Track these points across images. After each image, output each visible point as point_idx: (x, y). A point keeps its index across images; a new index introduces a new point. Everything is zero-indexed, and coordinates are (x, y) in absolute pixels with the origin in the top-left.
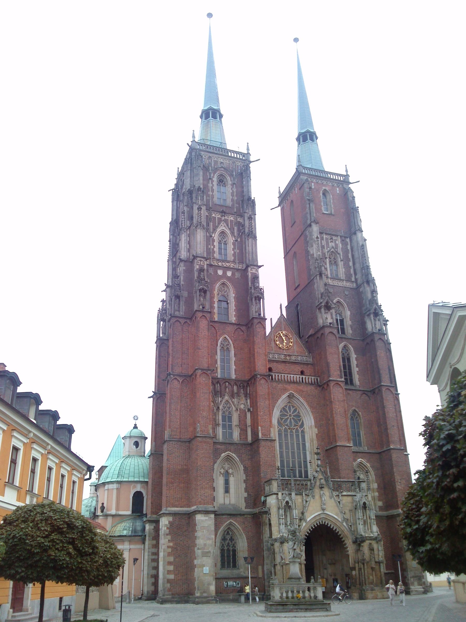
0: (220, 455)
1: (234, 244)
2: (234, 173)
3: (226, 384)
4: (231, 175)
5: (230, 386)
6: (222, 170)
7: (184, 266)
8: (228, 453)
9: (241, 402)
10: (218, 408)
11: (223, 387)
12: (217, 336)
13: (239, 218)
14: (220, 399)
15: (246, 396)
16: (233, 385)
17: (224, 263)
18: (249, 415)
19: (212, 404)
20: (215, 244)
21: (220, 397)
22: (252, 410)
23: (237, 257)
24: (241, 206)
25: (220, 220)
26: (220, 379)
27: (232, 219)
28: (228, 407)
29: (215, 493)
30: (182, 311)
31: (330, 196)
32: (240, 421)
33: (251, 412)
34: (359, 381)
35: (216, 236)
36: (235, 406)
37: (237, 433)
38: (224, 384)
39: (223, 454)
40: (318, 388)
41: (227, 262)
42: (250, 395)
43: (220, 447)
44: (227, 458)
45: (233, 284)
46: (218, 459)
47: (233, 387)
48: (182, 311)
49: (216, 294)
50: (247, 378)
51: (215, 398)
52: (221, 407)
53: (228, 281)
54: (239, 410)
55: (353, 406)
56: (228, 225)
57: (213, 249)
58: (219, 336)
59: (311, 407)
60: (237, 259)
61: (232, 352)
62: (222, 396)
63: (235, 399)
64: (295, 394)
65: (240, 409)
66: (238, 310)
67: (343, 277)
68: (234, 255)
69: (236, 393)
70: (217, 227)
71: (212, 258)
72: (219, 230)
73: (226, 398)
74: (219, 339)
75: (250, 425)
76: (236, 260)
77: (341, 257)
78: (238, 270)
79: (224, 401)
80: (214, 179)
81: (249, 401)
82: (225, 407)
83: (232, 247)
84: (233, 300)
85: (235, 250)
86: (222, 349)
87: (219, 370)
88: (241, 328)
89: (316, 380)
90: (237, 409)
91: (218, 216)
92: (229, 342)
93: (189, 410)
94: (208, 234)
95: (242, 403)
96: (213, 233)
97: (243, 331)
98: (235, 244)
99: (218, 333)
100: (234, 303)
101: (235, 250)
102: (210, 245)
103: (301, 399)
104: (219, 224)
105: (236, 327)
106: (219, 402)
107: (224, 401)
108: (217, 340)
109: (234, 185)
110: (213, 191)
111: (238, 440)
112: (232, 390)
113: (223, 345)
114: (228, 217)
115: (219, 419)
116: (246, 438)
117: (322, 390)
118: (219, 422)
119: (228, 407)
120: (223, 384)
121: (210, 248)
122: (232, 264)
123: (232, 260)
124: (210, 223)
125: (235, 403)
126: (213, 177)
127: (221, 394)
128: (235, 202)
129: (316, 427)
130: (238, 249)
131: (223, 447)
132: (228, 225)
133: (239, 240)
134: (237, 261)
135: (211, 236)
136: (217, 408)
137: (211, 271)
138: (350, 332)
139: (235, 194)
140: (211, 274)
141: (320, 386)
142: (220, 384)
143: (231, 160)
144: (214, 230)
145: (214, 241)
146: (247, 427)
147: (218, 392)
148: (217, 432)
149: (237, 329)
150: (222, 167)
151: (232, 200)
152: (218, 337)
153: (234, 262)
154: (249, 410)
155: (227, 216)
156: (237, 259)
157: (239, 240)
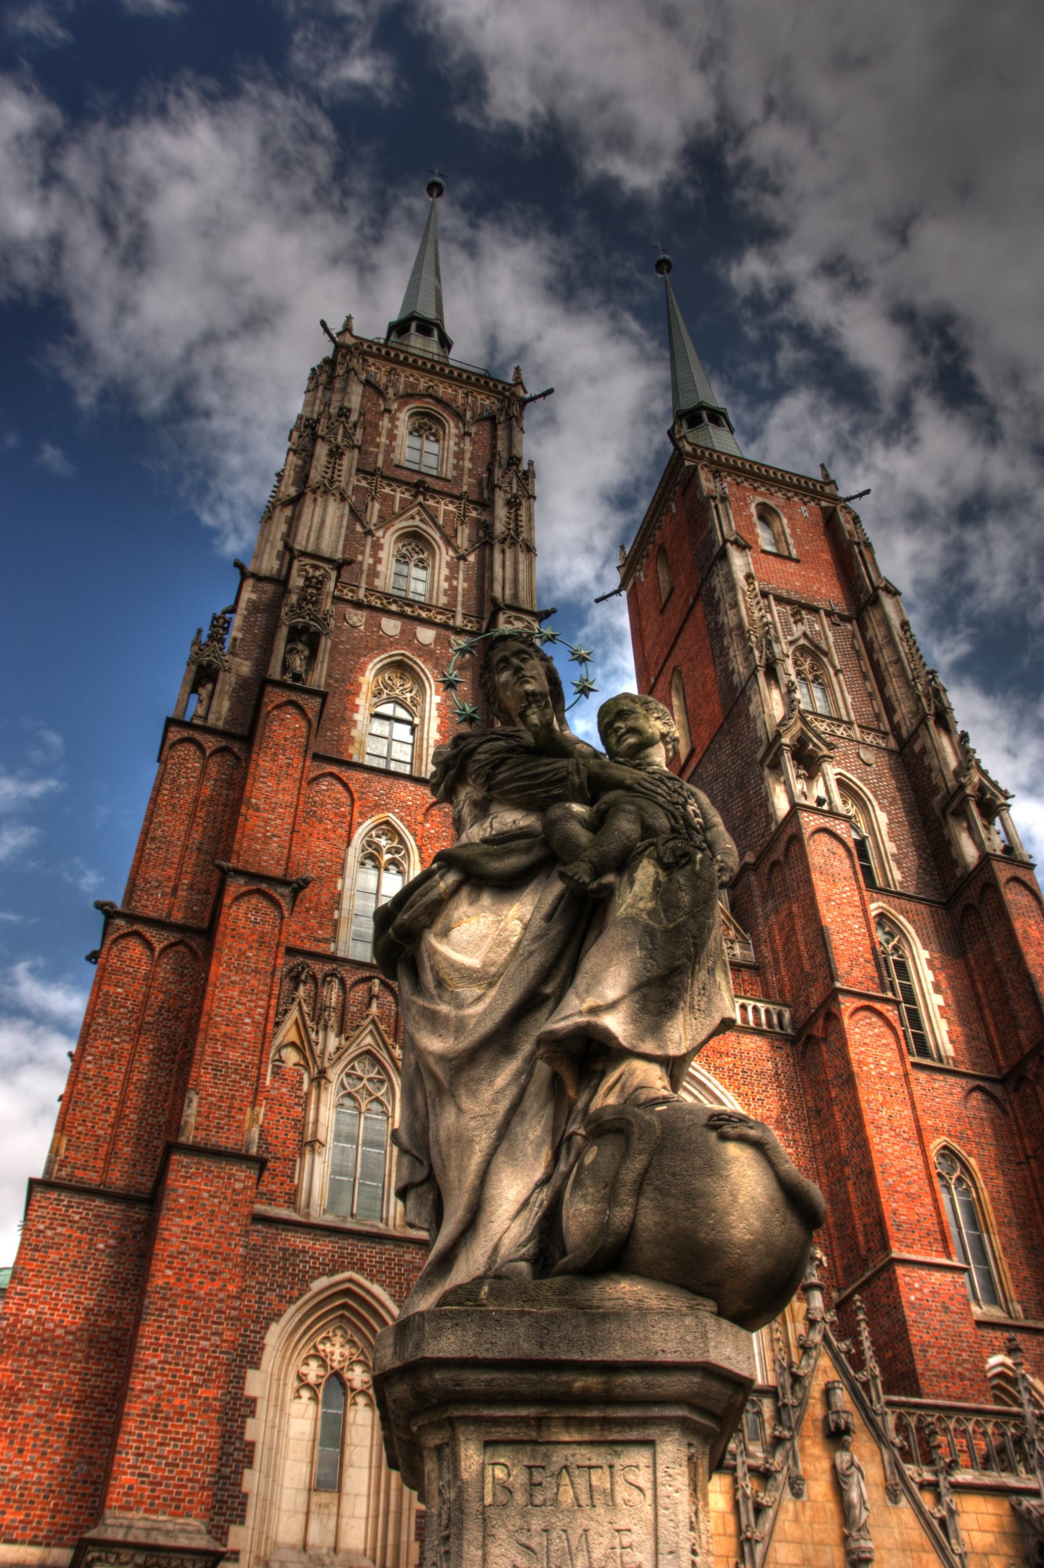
0: (305, 1280)
2: (469, 414)
3: (370, 989)
4: (459, 416)
8: (350, 1280)
10: (322, 1073)
12: (352, 814)
13: (475, 509)
14: (333, 1042)
19: (291, 1057)
20: (382, 554)
21: (339, 1035)
23: (460, 598)
25: (405, 507)
27: (451, 508)
29: (252, 1481)
34: (952, 1042)
38: (363, 987)
39: (323, 1282)
40: (787, 1049)
41: (421, 608)
44: (344, 1306)
46: (291, 1301)
49: (364, 688)
51: (313, 1036)
52: (334, 1074)
55: (937, 1131)
57: (372, 569)
71: (363, 585)
74: (360, 824)
76: (455, 606)
79: (353, 1051)
83: (445, 572)
84: (435, 713)
85: (455, 583)
91: (400, 495)
92: (402, 841)
94: (359, 528)
99: (357, 804)
101: (455, 583)
102: (363, 553)
104: (404, 509)
108: (350, 825)
110: (392, 437)
113: (378, 849)
117: (804, 1054)
118: (315, 1132)
119: (370, 1080)
120: (356, 984)
121: (361, 563)
122: (439, 617)
123: (440, 604)
126: (399, 410)
128: (466, 471)
131: (324, 1246)
132: (433, 519)
133: (472, 558)
134: (459, 609)
135: (369, 533)
136: (315, 1072)
137: (358, 618)
138: (898, 876)
139: (468, 455)
140: (355, 627)
141: (792, 1041)
142: (342, 982)
144: (385, 521)
145: (377, 546)
148: (301, 1178)
150: (430, 396)
151: (456, 467)
153: (449, 610)
155: (434, 498)
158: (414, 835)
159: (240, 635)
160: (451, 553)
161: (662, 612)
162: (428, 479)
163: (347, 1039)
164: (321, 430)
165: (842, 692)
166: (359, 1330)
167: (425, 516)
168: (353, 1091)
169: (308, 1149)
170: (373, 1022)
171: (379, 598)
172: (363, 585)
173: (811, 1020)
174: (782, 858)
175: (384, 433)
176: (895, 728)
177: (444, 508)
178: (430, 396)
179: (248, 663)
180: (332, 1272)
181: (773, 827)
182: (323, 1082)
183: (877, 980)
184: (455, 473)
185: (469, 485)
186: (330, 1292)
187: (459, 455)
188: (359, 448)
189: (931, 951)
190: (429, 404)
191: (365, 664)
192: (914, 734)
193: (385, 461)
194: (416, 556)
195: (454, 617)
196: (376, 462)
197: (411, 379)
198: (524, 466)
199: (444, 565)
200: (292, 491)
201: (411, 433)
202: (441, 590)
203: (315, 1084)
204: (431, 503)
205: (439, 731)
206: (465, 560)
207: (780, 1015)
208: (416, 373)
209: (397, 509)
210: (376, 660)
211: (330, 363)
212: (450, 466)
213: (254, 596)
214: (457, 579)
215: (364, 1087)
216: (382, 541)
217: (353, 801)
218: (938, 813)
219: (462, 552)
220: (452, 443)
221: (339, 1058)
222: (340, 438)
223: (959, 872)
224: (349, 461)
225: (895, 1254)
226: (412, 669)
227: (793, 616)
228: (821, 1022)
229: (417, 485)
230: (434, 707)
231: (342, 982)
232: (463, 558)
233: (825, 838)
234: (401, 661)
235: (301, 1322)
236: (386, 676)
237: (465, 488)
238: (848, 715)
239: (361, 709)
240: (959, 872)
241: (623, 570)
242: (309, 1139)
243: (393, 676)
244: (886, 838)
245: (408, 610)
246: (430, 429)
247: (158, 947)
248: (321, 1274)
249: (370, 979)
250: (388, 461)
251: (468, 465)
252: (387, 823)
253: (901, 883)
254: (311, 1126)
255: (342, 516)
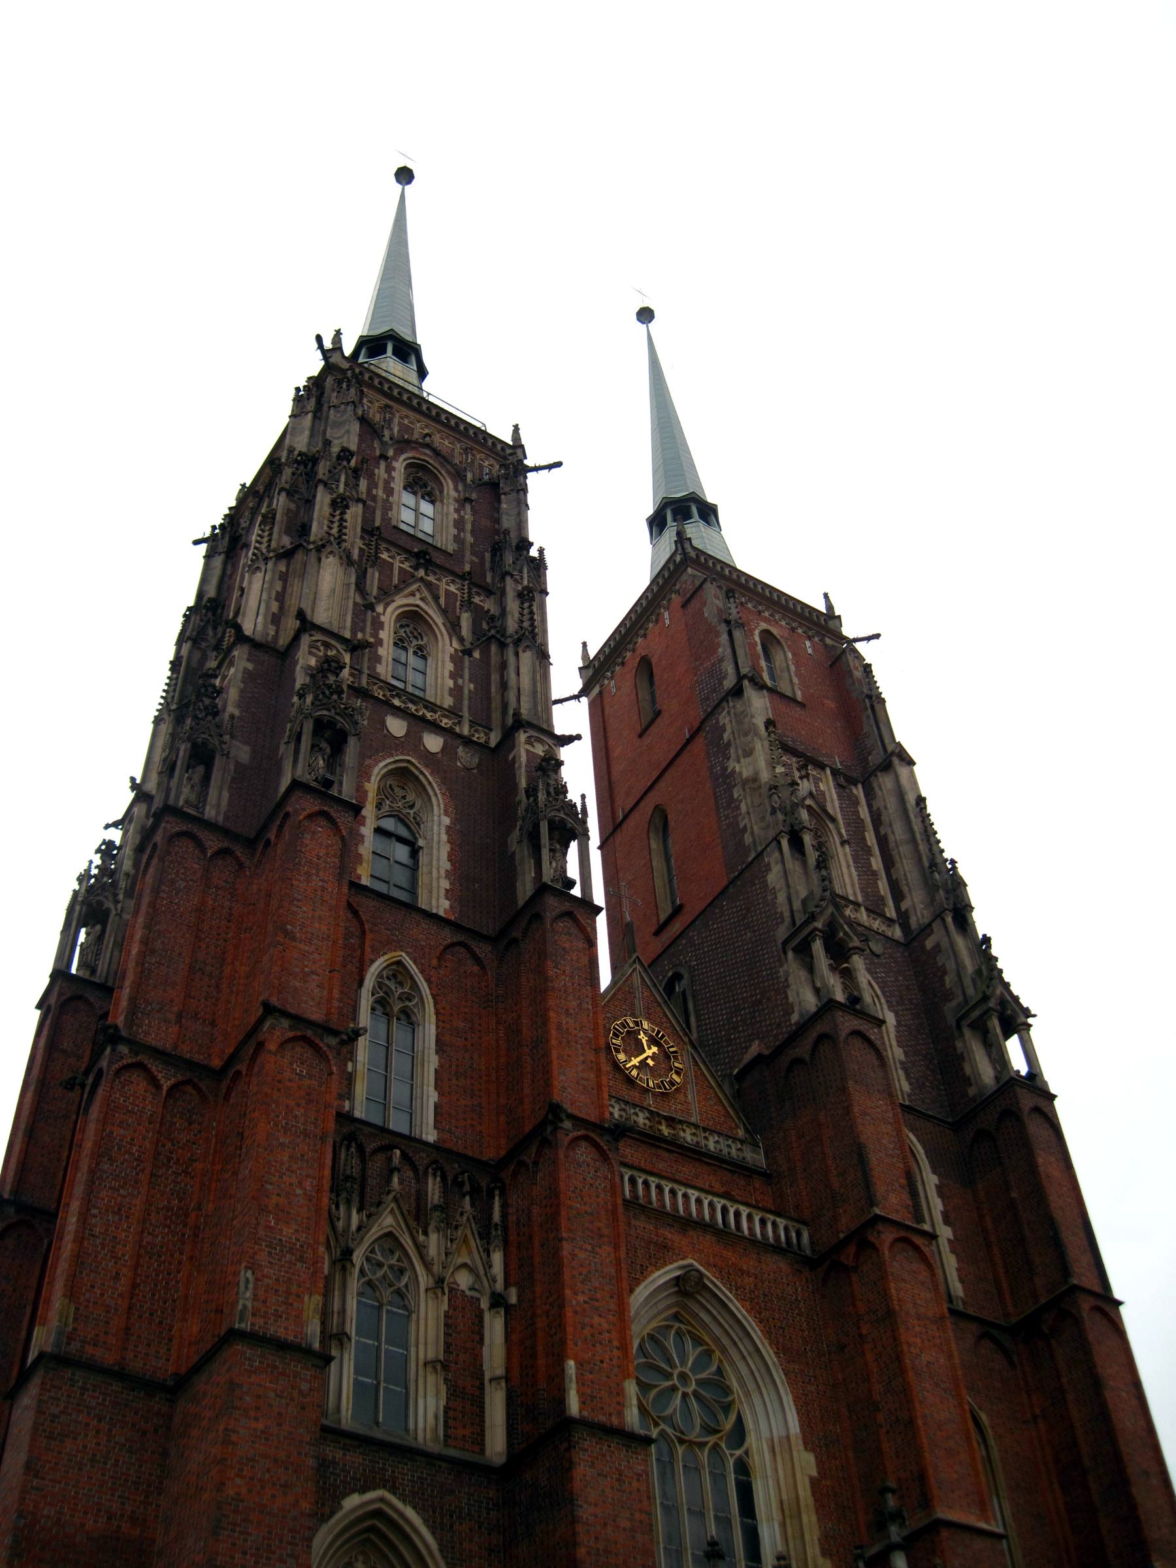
1: (456, 659)
2: (469, 476)
3: (390, 1159)
4: (458, 475)
5: (410, 1174)
6: (425, 454)
7: (248, 660)
8: (382, 1500)
9: (460, 1261)
11: (376, 1165)
15: (485, 1234)
16: (426, 1174)
17: (410, 705)
18: (495, 1328)
20: (383, 635)
21: (359, 1211)
22: (513, 1300)
23: (466, 702)
24: (488, 565)
25: (406, 579)
26: (367, 1130)
27: (452, 588)
28: (391, 1267)
30: (218, 805)
31: (785, 653)
32: (447, 1345)
33: (508, 1308)
35: (389, 615)
36: (427, 1265)
37: (431, 1401)
38: (380, 1157)
39: (353, 1501)
41: (426, 707)
42: (505, 1229)
43: (339, 1455)
44: (372, 1529)
45: (444, 782)
47: (420, 1179)
48: (218, 805)
50: (490, 1153)
53: (427, 766)
54: (446, 1291)
56: (436, 598)
58: (372, 947)
59: (782, 1349)
60: (465, 709)
61: (429, 1030)
62: (369, 1207)
63: (433, 1237)
64: (711, 1278)
65: (451, 1290)
66: (461, 874)
67: (855, 894)
68: (456, 692)
69: (435, 1208)
70: (398, 589)
71: (366, 671)
72: (401, 601)
73: (387, 1221)
74: (373, 961)
75: (500, 1371)
76: (461, 710)
77: (843, 831)
78: (467, 742)
79: (375, 1232)
80: (395, 464)
81: (497, 1258)
82: (380, 1265)
83: (450, 666)
84: (444, 837)
85: (460, 681)
86: (378, 1007)
87: (360, 1089)
88: (473, 944)
89: (794, 1235)
90: (440, 1281)
91: (399, 564)
92: (415, 986)
93: (188, 1232)
95: (465, 1265)
96: (378, 599)
97: (477, 960)
98: (462, 661)
99: (369, 936)
100: (445, 849)
103: (736, 1306)
105: (447, 936)
106: (354, 1226)
107: (375, 1232)
109: (468, 507)
111: (436, 1439)
112: (418, 1192)
114: (439, 580)
115: (343, 1311)
116: (479, 1439)
119: (391, 1267)
120: (375, 1152)
122: (445, 721)
123: (446, 706)
124: (370, 570)
125: (433, 1251)
126: (395, 458)
127: (362, 1195)
128: (468, 547)
129: (808, 1444)
130: (470, 681)
131: (354, 1459)
132: (436, 598)
134: (466, 713)
139: (469, 527)
142: (361, 1149)
143: (459, 441)
144: (386, 593)
146: (481, 1387)
147: (348, 1178)
149: (453, 945)
150: (428, 446)
151: (457, 539)
152: (368, 950)
153: (454, 712)
154: (498, 1301)
155: (435, 573)
156: (465, 709)
157: (476, 655)
158: (428, 980)
159: (237, 713)
160: (456, 644)
161: (640, 736)
162: (430, 550)
163: (369, 1216)
164: (322, 470)
165: (848, 867)
166: (385, 1556)
167: (426, 593)
168: (373, 1278)
169: (334, 1343)
170: (395, 1199)
171: (381, 688)
172: (366, 671)
173: (842, 1245)
174: (807, 1057)
175: (381, 484)
176: (903, 918)
177: (448, 586)
178: (428, 446)
179: (247, 748)
180: (363, 1490)
181: (795, 1018)
182: (348, 1265)
183: (911, 1209)
184: (456, 547)
185: (472, 563)
186: (360, 1512)
187: (459, 524)
188: (364, 503)
189: (940, 1175)
190: (426, 456)
191: (371, 767)
192: (926, 929)
193: (383, 520)
194: (415, 643)
195: (459, 723)
196: (373, 521)
197: (406, 421)
198: (534, 552)
199: (447, 659)
200: (287, 541)
201: (405, 488)
202: (447, 689)
203: (338, 1266)
204: (431, 578)
205: (450, 860)
206: (470, 655)
207: (799, 1234)
208: (411, 414)
209: (396, 580)
210: (381, 765)
211: (316, 385)
212: (451, 538)
213: (250, 666)
214: (462, 677)
215: (384, 1277)
216: (382, 618)
217: (363, 932)
218: (951, 1020)
219: (468, 646)
220: (452, 508)
221: (362, 1239)
222: (342, 486)
223: (972, 1091)
224: (354, 514)
225: (943, 1513)
226: (417, 778)
227: (798, 770)
228: (852, 1250)
229: (417, 555)
230: (443, 831)
231: (361, 1149)
232: (468, 652)
233: (857, 1042)
234: (405, 768)
235: (331, 1545)
236: (388, 783)
237: (467, 568)
238: (855, 894)
239: (368, 821)
240: (972, 1091)
241: (590, 672)
242: (335, 1331)
243: (394, 784)
244: (894, 1043)
245: (413, 708)
246: (425, 486)
247: (166, 1085)
248: (353, 1491)
249: (390, 1147)
250: (386, 520)
251: (469, 539)
252: (399, 963)
253: (909, 1096)
254: (336, 1316)
255: (348, 585)
